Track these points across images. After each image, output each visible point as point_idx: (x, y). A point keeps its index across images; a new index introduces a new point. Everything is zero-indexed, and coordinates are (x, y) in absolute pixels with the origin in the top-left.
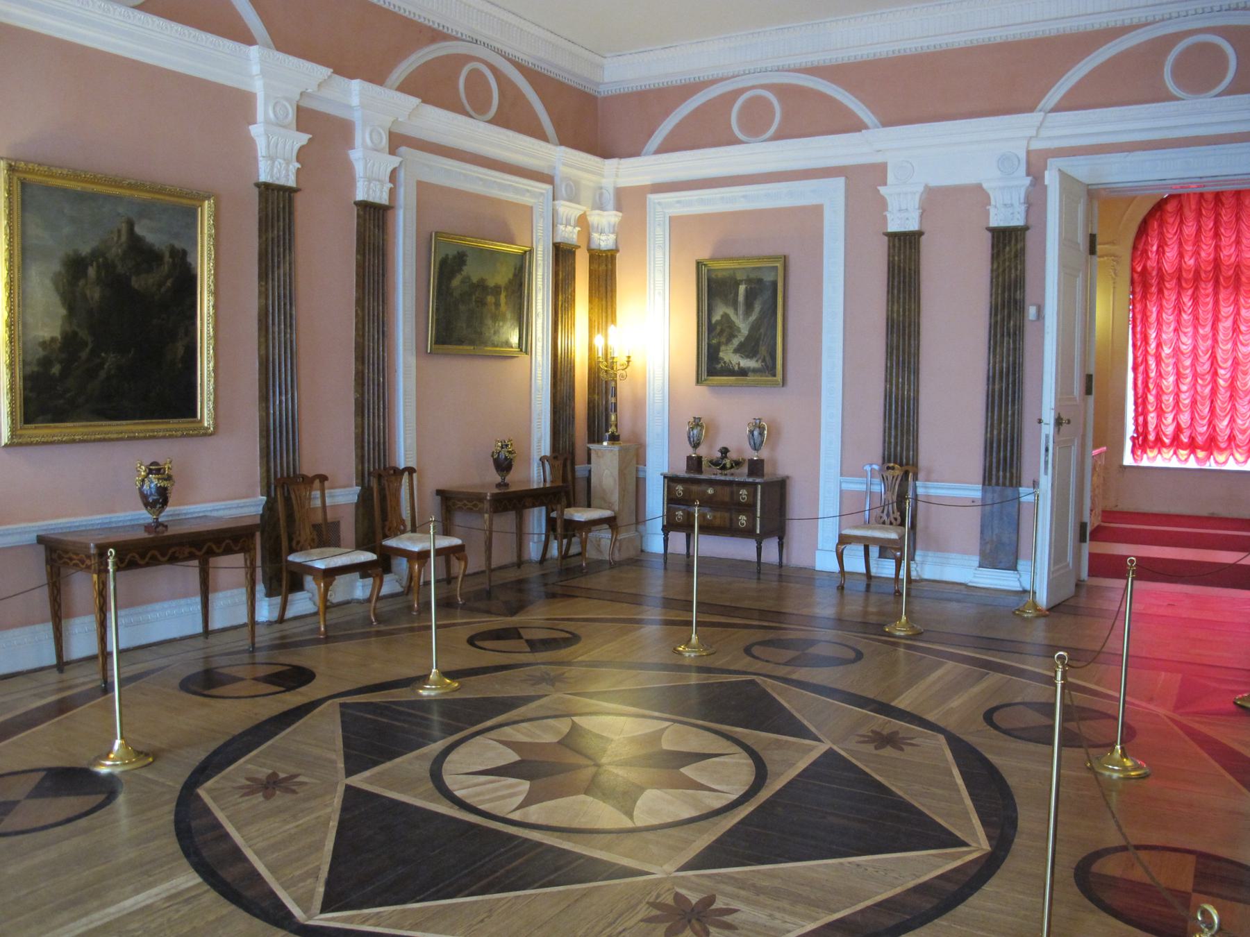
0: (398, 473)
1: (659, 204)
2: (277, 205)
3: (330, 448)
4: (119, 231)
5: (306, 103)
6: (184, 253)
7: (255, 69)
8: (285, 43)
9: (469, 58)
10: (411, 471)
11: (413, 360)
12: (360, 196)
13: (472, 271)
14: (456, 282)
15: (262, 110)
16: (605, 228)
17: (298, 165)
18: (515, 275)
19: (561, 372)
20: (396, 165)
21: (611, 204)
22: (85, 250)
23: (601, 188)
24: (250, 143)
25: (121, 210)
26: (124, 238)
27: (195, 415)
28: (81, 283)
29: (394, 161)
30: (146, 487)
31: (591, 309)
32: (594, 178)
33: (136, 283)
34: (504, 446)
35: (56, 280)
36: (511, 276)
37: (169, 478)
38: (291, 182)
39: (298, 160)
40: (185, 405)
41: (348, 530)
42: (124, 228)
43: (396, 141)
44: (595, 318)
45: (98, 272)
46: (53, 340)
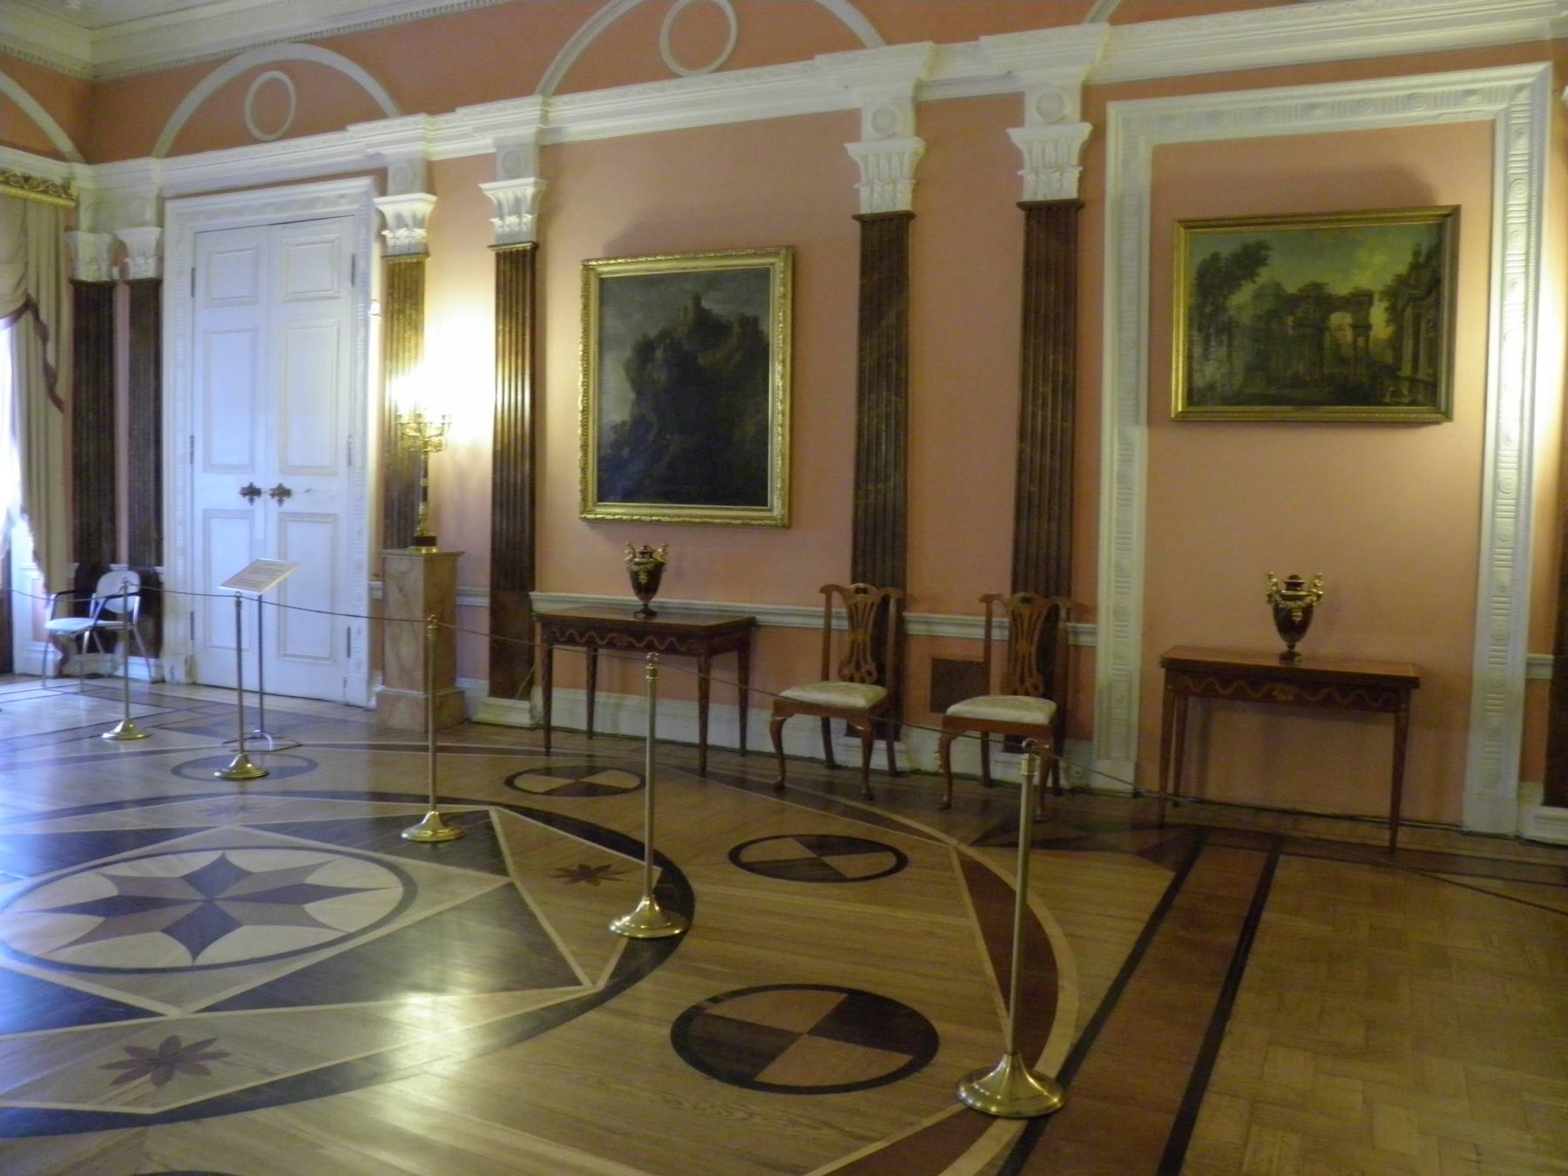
2: (886, 244)
8: (892, 34)
11: (1139, 435)
13: (1287, 273)
14: (1242, 301)
18: (1415, 267)
22: (653, 333)
25: (688, 286)
26: (691, 315)
28: (650, 366)
33: (703, 360)
34: (1294, 584)
35: (628, 369)
36: (1402, 268)
40: (756, 494)
42: (690, 303)
46: (624, 423)
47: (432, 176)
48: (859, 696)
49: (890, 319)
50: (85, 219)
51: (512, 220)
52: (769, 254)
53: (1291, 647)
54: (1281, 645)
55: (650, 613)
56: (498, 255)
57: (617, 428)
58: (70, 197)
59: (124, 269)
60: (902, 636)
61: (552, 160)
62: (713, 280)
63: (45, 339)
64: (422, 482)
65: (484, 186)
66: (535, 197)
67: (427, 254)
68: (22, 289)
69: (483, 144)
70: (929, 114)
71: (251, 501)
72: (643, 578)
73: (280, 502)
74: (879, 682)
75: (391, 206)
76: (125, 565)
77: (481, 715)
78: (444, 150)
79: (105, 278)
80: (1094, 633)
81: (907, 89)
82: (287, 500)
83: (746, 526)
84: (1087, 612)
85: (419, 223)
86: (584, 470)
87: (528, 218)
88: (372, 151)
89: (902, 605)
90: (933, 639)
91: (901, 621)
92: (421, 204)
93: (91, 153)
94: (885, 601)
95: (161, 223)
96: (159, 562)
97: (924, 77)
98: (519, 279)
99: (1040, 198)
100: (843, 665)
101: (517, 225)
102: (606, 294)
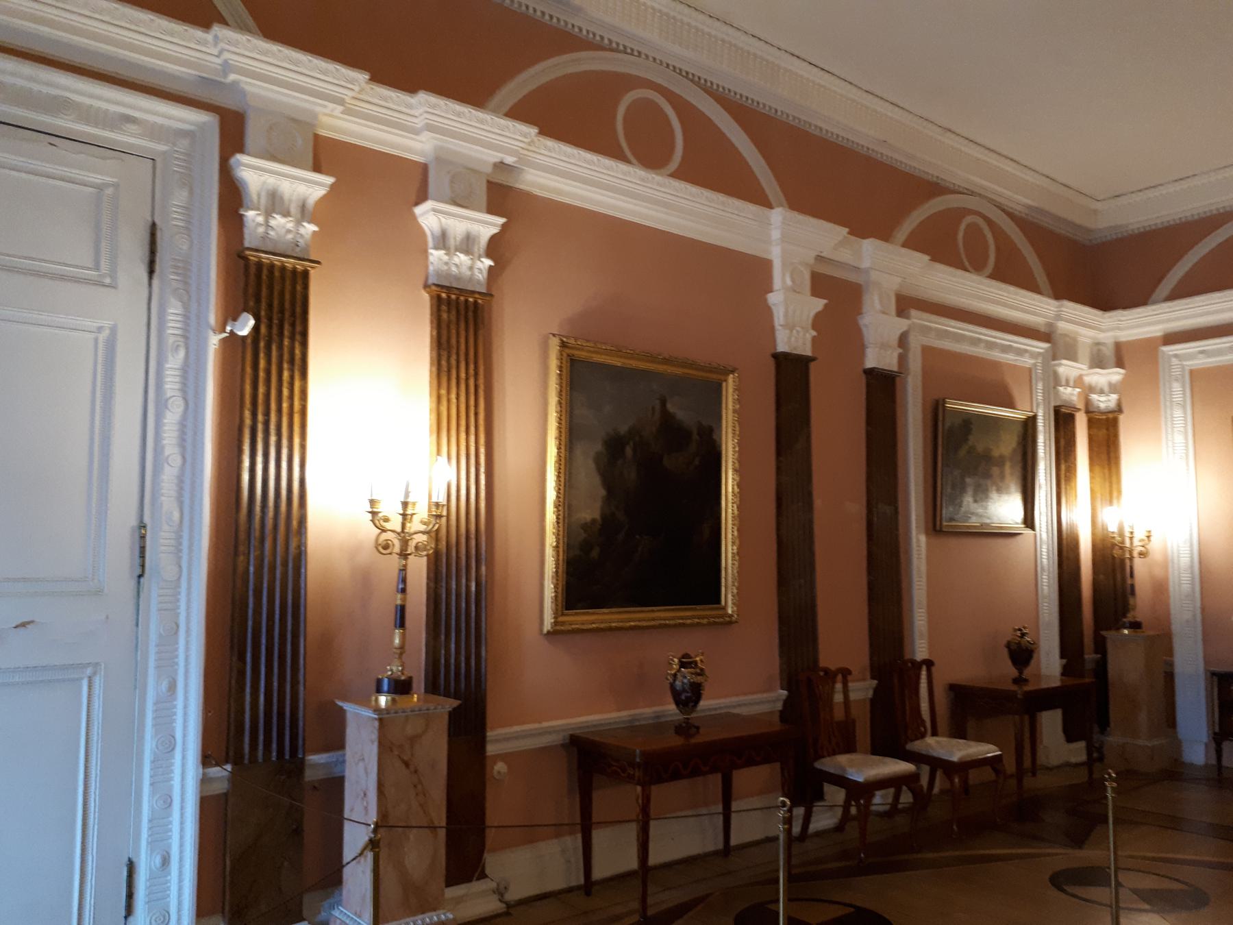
0: (917, 666)
1: (1176, 356)
3: (842, 639)
4: (653, 408)
7: (776, 234)
9: (967, 212)
10: (929, 663)
11: (923, 538)
12: (870, 363)
15: (779, 278)
16: (1103, 384)
17: (814, 333)
19: (1066, 547)
20: (905, 328)
21: (1112, 359)
22: (623, 429)
23: (1098, 344)
24: (768, 312)
27: (719, 602)
29: (903, 324)
30: (678, 683)
31: (1092, 478)
32: (1091, 333)
35: (597, 460)
37: (701, 673)
38: (807, 351)
39: (814, 327)
41: (863, 733)
43: (905, 304)
44: (1097, 489)
46: (594, 521)
51: (462, 258)
53: (1021, 673)
54: (1013, 672)
57: (585, 527)
102: (582, 377)
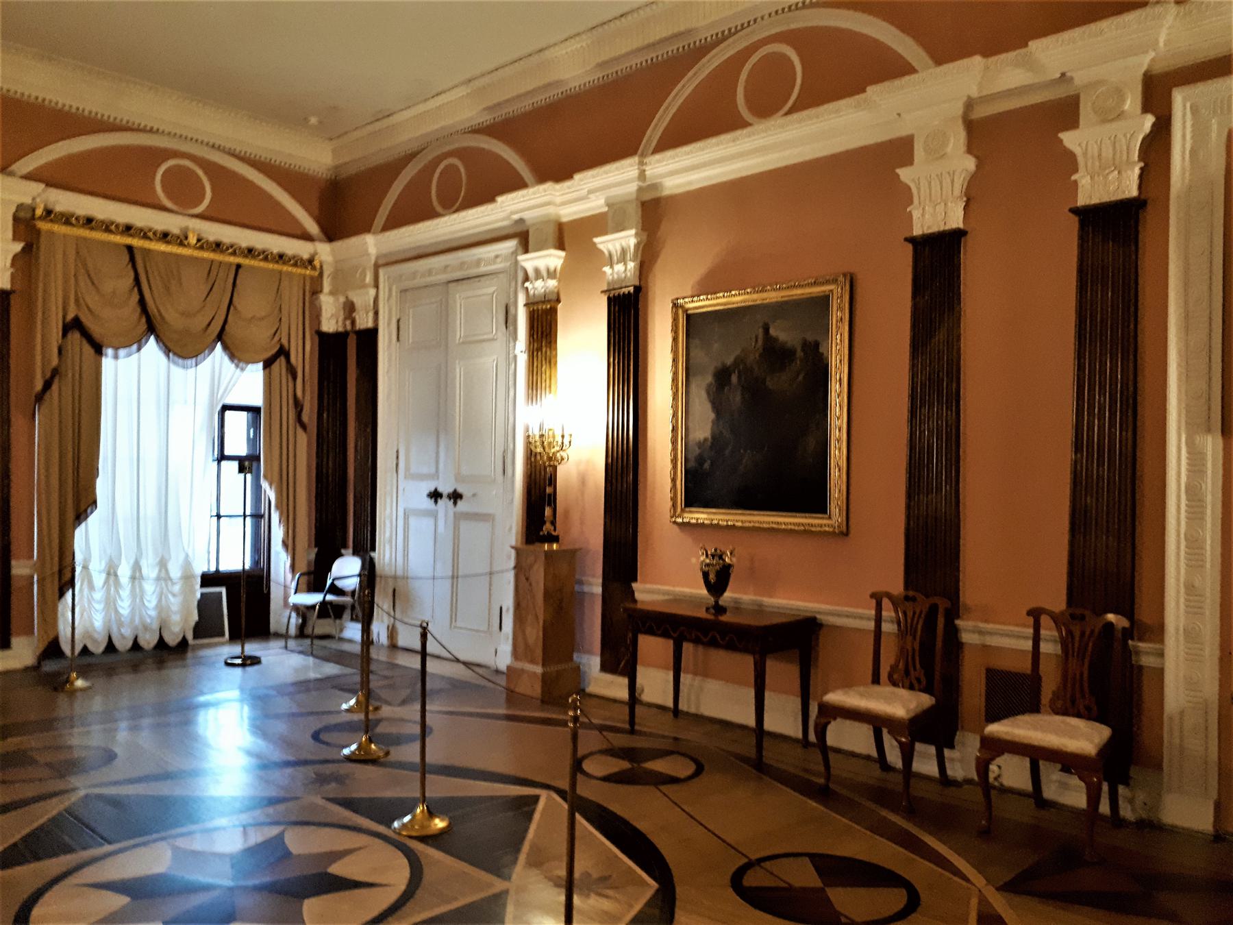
5: (980, 113)
6: (817, 345)
22: (729, 361)
40: (818, 504)
45: (739, 377)
46: (706, 440)
47: (562, 235)
48: (899, 704)
49: (941, 336)
50: (327, 286)
51: (619, 268)
52: (827, 282)
55: (719, 609)
56: (609, 298)
57: (700, 445)
58: (314, 268)
59: (353, 323)
60: (954, 644)
61: (653, 212)
62: (781, 310)
63: (295, 378)
64: (549, 490)
65: (596, 240)
66: (637, 246)
67: (558, 301)
68: (276, 338)
69: (596, 205)
70: (982, 131)
71: (436, 502)
72: (712, 577)
73: (455, 503)
74: (927, 690)
75: (530, 262)
76: (351, 550)
77: (592, 689)
78: (568, 213)
79: (341, 329)
80: (1161, 654)
81: (959, 109)
82: (459, 503)
83: (807, 533)
84: (1157, 632)
85: (551, 274)
86: (674, 480)
87: (631, 265)
88: (516, 217)
89: (954, 612)
90: (985, 647)
91: (953, 633)
92: (553, 259)
93: (332, 233)
94: (933, 609)
95: (377, 286)
96: (373, 549)
97: (974, 93)
98: (626, 316)
99: (1095, 200)
100: (893, 668)
101: (623, 272)
102: (694, 327)
